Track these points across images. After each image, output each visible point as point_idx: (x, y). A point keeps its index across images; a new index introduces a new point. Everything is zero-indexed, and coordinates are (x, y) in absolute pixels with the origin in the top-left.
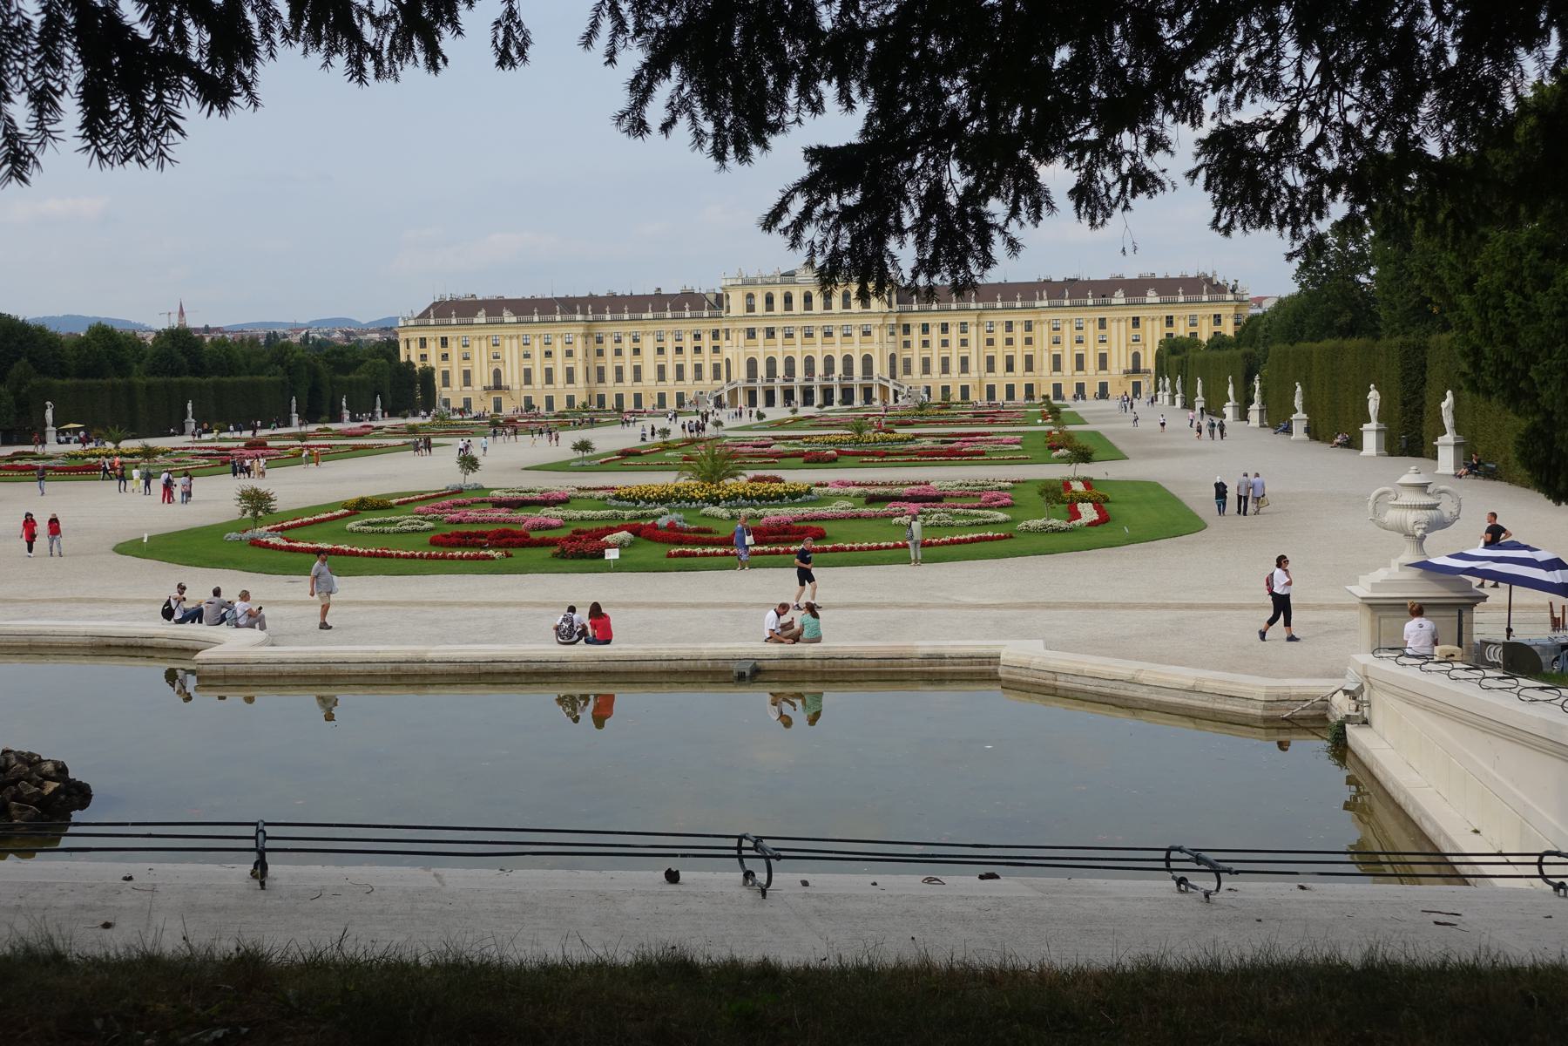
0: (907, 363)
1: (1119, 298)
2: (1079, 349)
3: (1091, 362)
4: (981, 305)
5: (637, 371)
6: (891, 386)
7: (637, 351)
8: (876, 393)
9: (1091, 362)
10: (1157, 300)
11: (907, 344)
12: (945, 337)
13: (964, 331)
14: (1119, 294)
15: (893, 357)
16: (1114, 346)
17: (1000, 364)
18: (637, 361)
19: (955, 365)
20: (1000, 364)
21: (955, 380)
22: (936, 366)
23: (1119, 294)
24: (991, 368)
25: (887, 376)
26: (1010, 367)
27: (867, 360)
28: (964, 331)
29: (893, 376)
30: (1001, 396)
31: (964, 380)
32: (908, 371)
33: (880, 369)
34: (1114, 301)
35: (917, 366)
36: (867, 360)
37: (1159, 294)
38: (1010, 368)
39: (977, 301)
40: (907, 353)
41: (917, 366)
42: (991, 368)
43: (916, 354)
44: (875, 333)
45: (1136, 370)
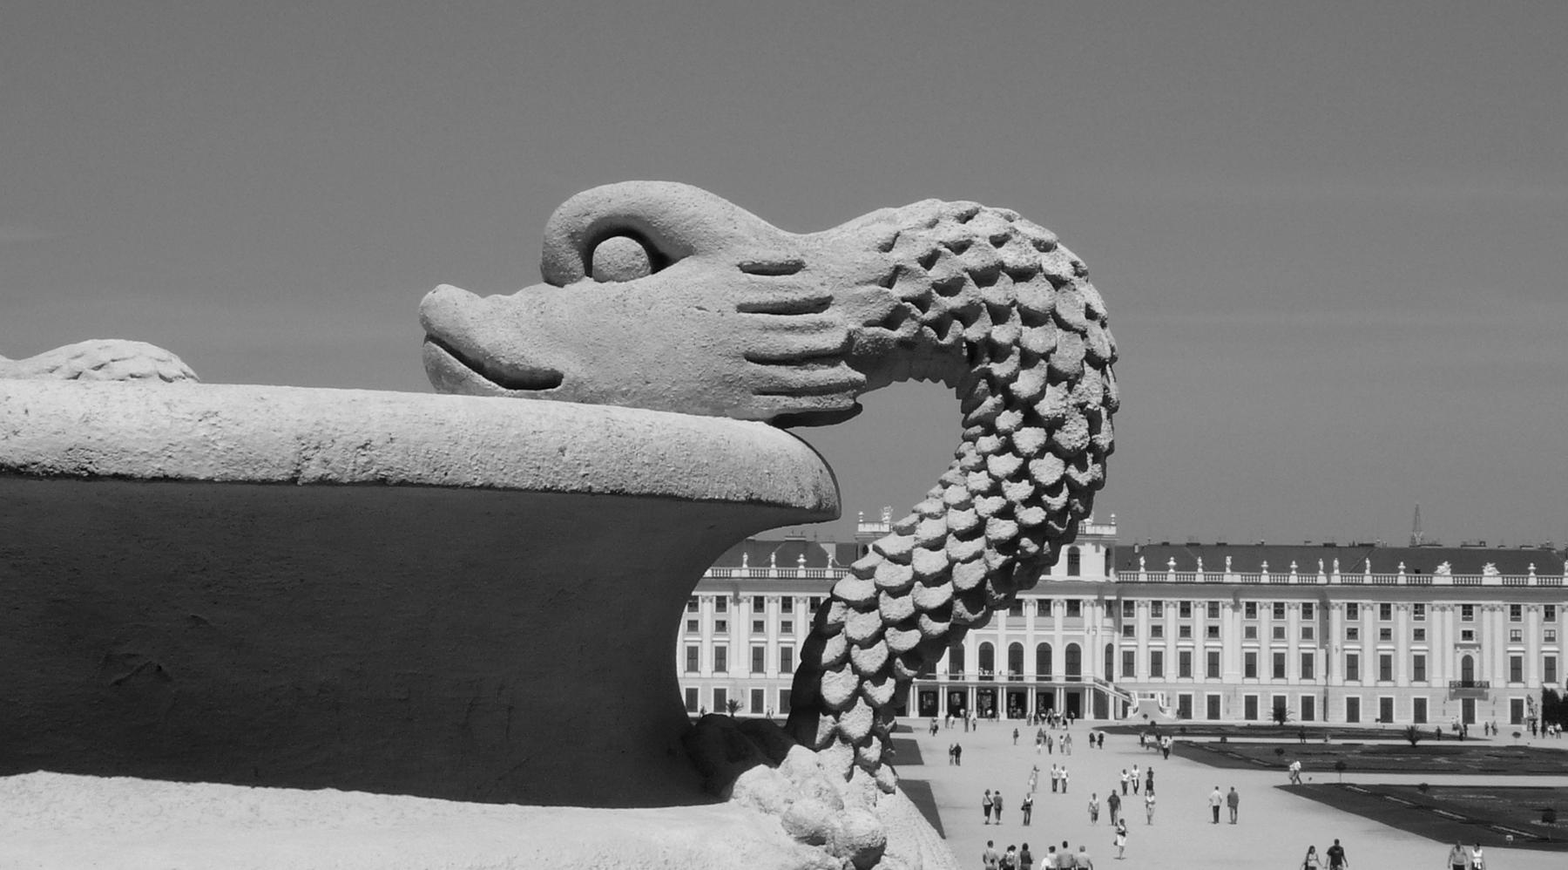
0: (1129, 659)
1: (1444, 575)
2: (1385, 647)
3: (1402, 669)
4: (1237, 578)
5: (721, 656)
6: (1110, 690)
7: (721, 626)
8: (1088, 701)
9: (1402, 669)
10: (1498, 581)
11: (1129, 631)
12: (1185, 622)
13: (1157, 614)
14: (1444, 568)
15: (1109, 650)
16: (1436, 646)
17: (1265, 667)
18: (721, 640)
19: (1199, 665)
20: (1265, 667)
21: (1199, 684)
22: (1171, 665)
23: (1444, 568)
24: (1251, 671)
25: (1102, 677)
26: (1279, 671)
27: (1073, 654)
28: (1157, 614)
29: (1109, 677)
30: (1200, 716)
31: (1214, 687)
32: (1129, 668)
33: (1092, 669)
34: (1437, 580)
35: (1143, 664)
36: (1073, 654)
37: (1503, 570)
38: (1279, 671)
39: (1234, 569)
40: (1128, 644)
41: (1143, 664)
42: (1251, 671)
43: (1142, 646)
44: (1086, 611)
45: (1467, 682)
